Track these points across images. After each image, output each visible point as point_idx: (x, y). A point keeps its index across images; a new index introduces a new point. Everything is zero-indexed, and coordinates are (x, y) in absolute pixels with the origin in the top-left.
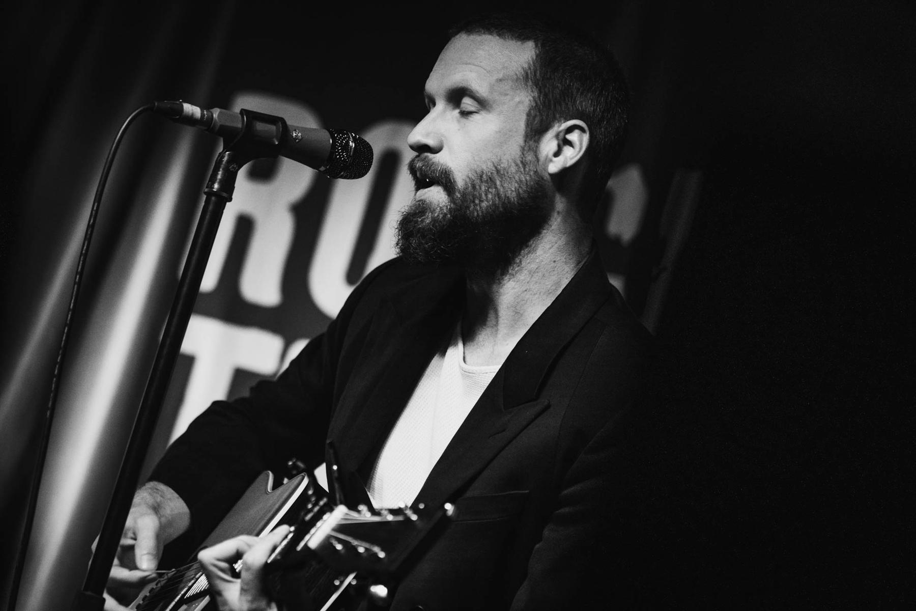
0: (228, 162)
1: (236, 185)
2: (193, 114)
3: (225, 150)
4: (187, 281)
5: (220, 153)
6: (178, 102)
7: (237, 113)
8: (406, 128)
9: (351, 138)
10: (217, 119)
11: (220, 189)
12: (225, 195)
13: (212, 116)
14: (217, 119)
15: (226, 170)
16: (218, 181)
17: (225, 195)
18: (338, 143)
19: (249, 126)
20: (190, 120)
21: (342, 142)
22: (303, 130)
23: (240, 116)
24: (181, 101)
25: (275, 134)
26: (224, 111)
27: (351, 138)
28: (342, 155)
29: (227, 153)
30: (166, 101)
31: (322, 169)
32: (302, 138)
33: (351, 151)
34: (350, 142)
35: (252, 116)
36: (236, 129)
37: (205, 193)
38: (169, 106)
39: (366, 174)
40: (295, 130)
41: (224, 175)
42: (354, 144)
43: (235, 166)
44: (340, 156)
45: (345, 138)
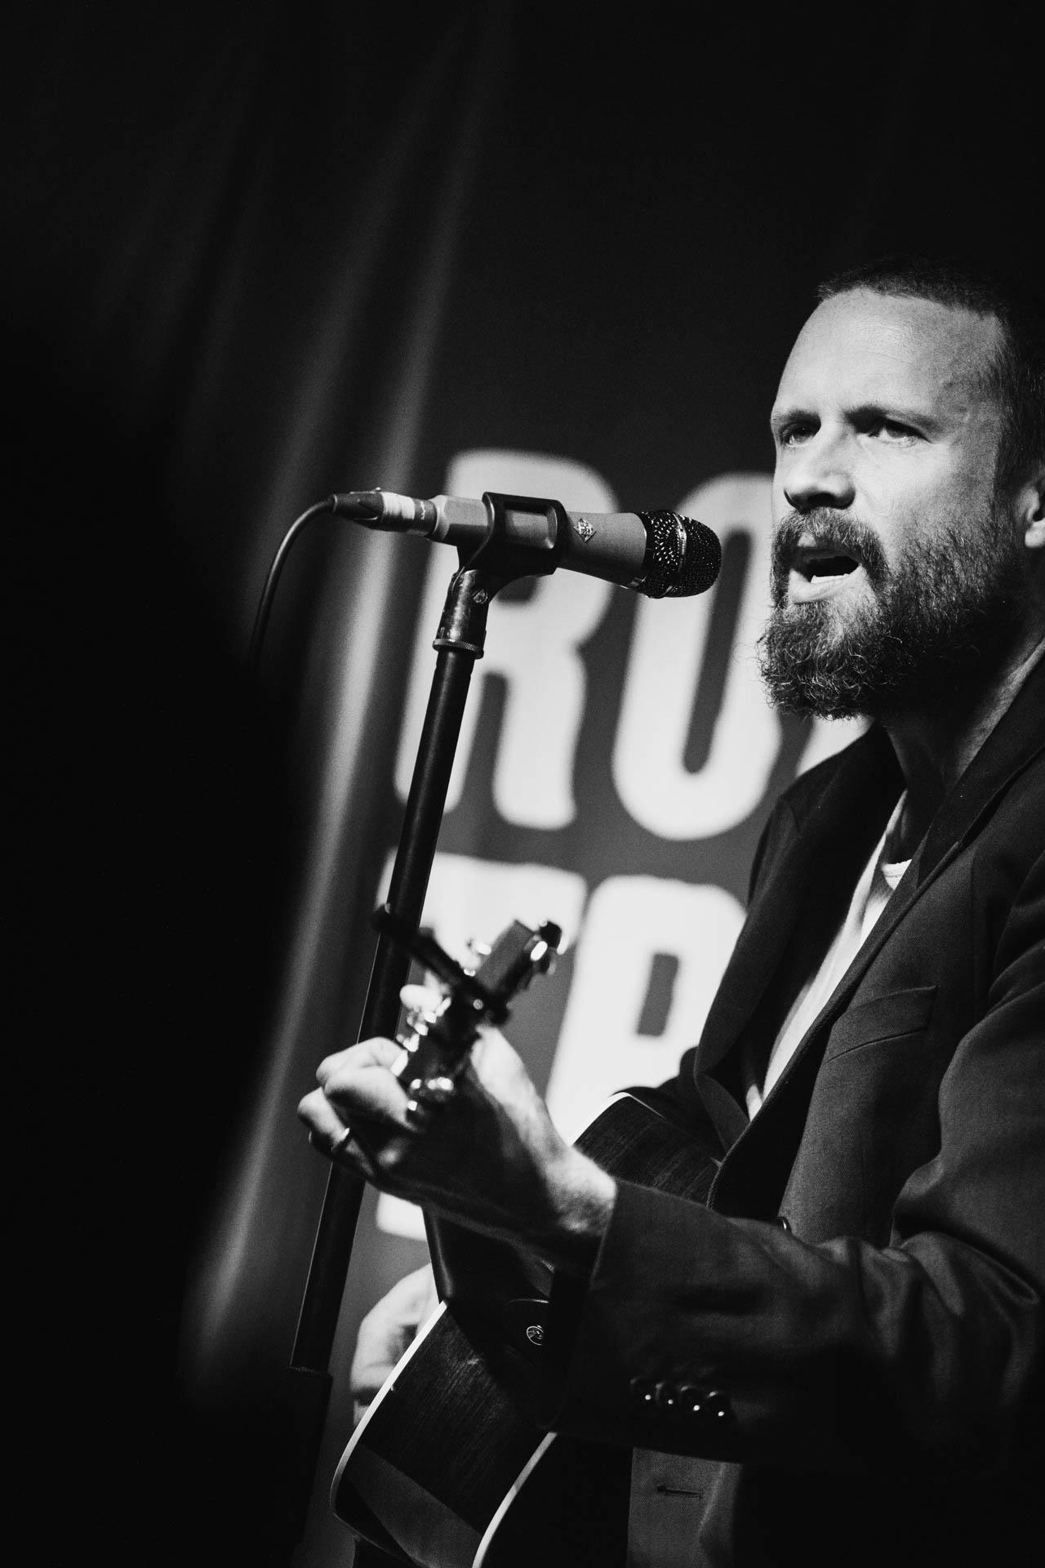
0: (473, 588)
2: (401, 513)
4: (420, 805)
6: (372, 492)
9: (679, 522)
10: (443, 513)
12: (470, 647)
15: (469, 602)
17: (470, 647)
18: (658, 534)
19: (501, 521)
20: (395, 523)
24: (378, 489)
25: (547, 531)
27: (679, 522)
29: (468, 573)
30: (352, 493)
34: (679, 530)
35: (502, 504)
36: (481, 527)
37: (435, 647)
38: (359, 500)
40: (581, 520)
44: (662, 555)
45: (670, 524)
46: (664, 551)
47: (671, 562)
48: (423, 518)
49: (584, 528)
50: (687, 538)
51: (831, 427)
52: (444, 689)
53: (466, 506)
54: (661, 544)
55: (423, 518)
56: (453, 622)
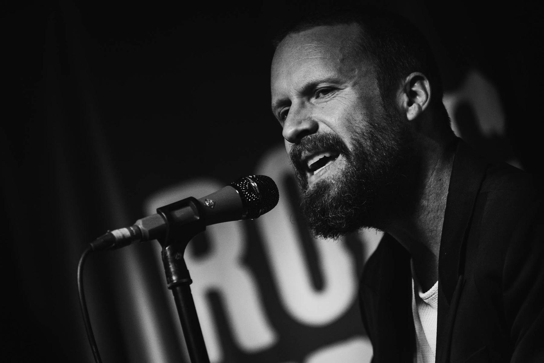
0: (172, 254)
2: (124, 236)
3: (164, 247)
5: (162, 252)
6: (107, 234)
7: (156, 214)
8: (420, 89)
9: (250, 179)
10: (143, 228)
11: (179, 279)
12: (184, 280)
13: (138, 228)
14: (143, 228)
15: (175, 262)
16: (173, 273)
17: (184, 280)
18: (243, 190)
19: (170, 219)
20: (124, 241)
21: (245, 187)
22: (210, 197)
23: (159, 215)
26: (144, 219)
27: (250, 179)
28: (252, 196)
29: (167, 248)
30: (98, 239)
31: (244, 216)
32: (215, 203)
33: (256, 190)
34: (252, 183)
36: (164, 224)
37: (169, 288)
39: (279, 200)
40: (206, 200)
41: (175, 266)
42: (255, 184)
43: (179, 254)
44: (250, 198)
45: (246, 183)
47: (255, 199)
48: (135, 234)
49: (209, 203)
50: (257, 185)
51: (295, 101)
52: (182, 305)
54: (247, 193)
55: (135, 234)
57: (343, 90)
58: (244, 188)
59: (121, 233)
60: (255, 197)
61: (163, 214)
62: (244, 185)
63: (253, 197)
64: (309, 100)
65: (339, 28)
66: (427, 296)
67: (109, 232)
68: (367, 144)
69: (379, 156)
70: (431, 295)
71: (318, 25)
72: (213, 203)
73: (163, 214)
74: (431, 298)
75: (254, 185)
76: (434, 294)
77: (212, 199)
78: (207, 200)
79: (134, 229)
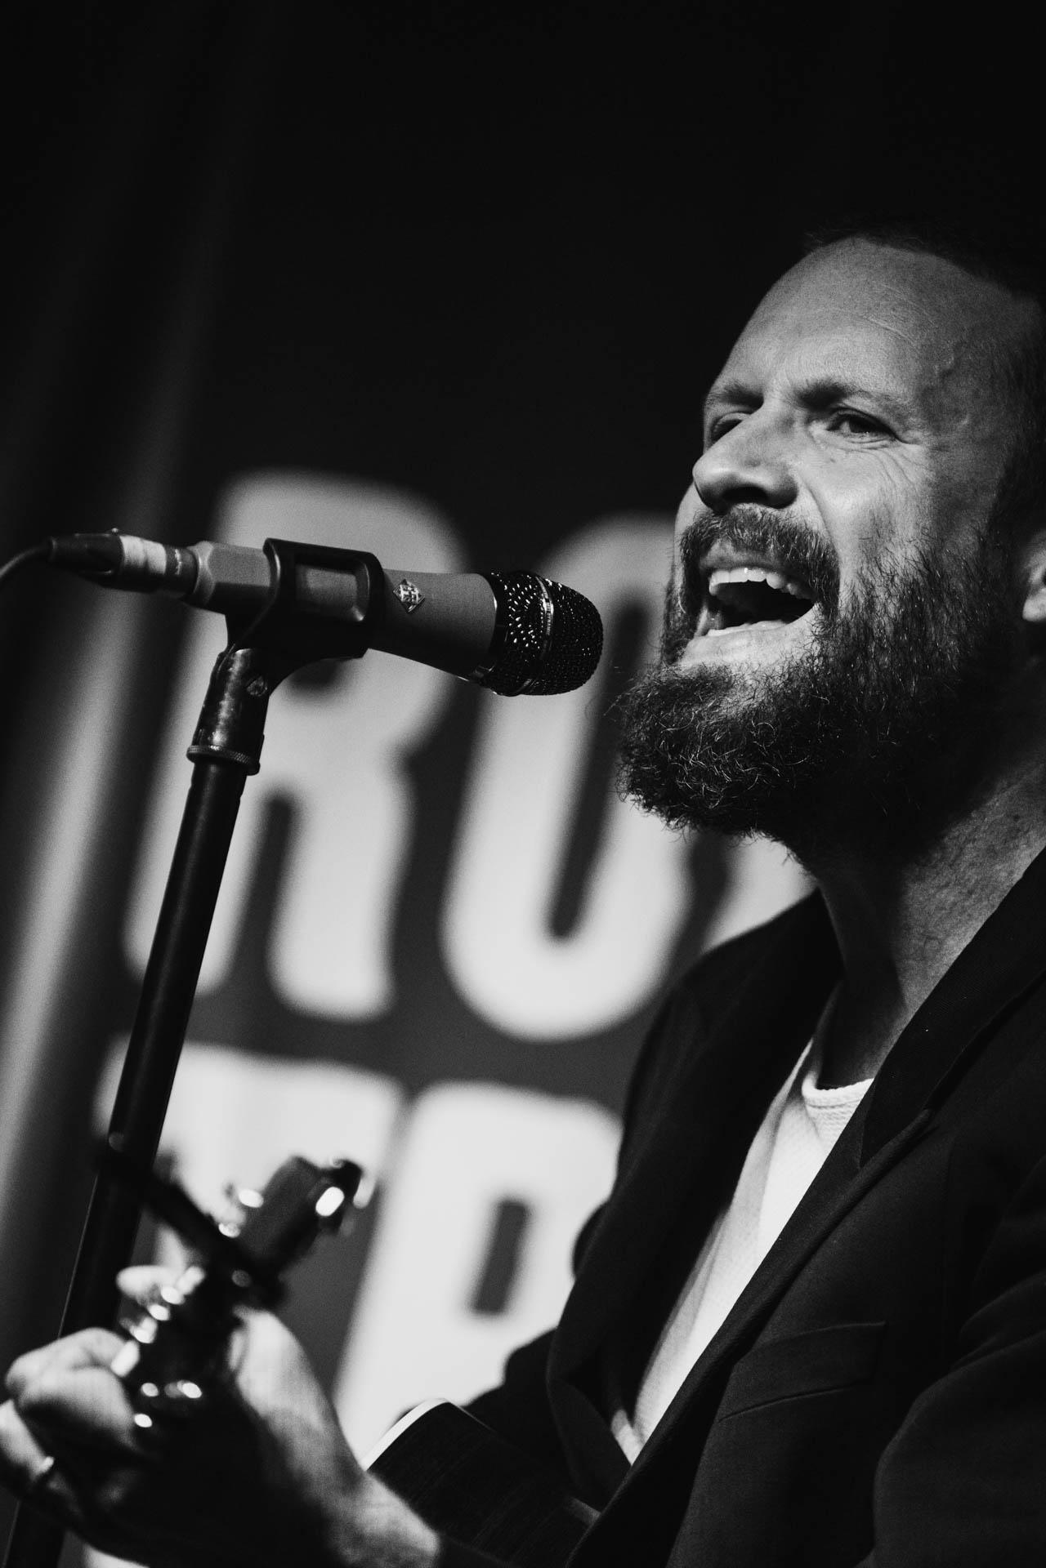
0: (247, 675)
1: (266, 732)
2: (146, 563)
5: (222, 656)
6: (107, 535)
9: (543, 588)
12: (240, 757)
15: (241, 696)
16: (221, 723)
17: (240, 757)
18: (513, 606)
19: (289, 582)
20: (140, 578)
21: (522, 602)
22: (421, 578)
25: (354, 595)
27: (543, 588)
28: (526, 634)
29: (240, 652)
30: (77, 535)
33: (546, 623)
34: (544, 600)
37: (191, 756)
38: (86, 546)
40: (404, 582)
42: (552, 606)
44: (520, 638)
45: (530, 592)
46: (521, 629)
48: (178, 573)
49: (407, 593)
50: (554, 612)
51: (774, 405)
52: (202, 817)
53: (242, 557)
54: (517, 619)
55: (178, 573)
56: (217, 721)
57: (903, 444)
58: (516, 602)
59: (145, 552)
60: (534, 640)
61: (277, 559)
62: (521, 595)
63: (529, 637)
64: (808, 421)
65: (985, 292)
66: (821, 1102)
67: (116, 534)
68: (889, 608)
69: (900, 656)
70: (831, 1104)
71: (938, 253)
72: (417, 598)
73: (277, 559)
74: (830, 1111)
75: (546, 609)
76: (841, 1106)
77: (420, 588)
78: (408, 583)
79: (182, 560)
